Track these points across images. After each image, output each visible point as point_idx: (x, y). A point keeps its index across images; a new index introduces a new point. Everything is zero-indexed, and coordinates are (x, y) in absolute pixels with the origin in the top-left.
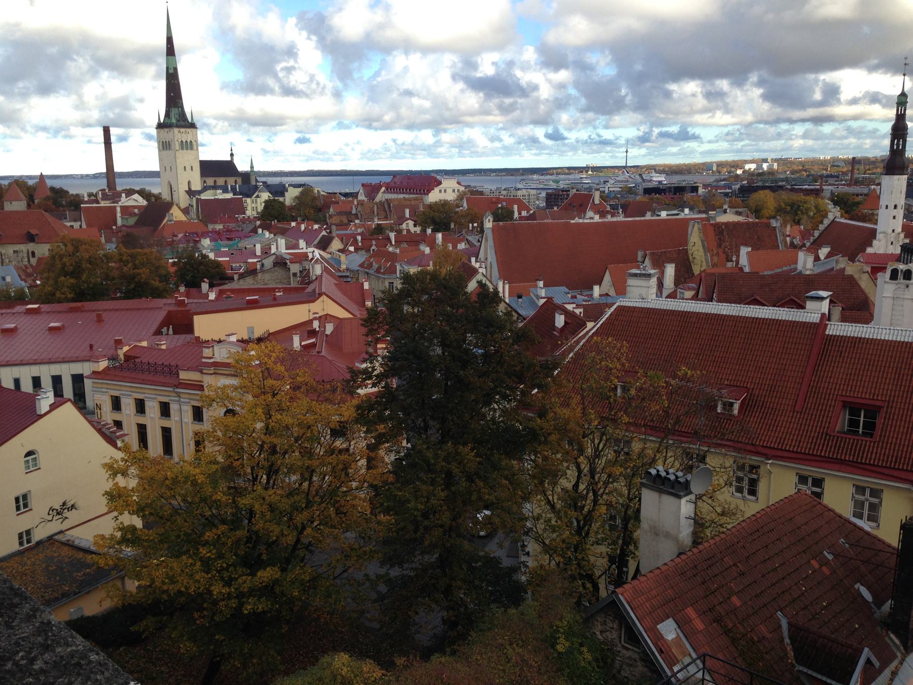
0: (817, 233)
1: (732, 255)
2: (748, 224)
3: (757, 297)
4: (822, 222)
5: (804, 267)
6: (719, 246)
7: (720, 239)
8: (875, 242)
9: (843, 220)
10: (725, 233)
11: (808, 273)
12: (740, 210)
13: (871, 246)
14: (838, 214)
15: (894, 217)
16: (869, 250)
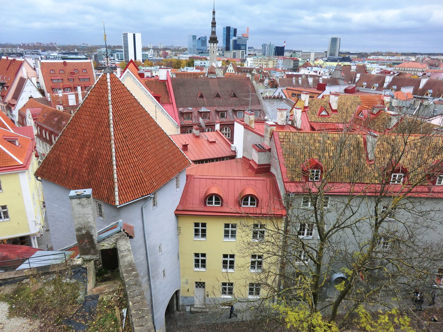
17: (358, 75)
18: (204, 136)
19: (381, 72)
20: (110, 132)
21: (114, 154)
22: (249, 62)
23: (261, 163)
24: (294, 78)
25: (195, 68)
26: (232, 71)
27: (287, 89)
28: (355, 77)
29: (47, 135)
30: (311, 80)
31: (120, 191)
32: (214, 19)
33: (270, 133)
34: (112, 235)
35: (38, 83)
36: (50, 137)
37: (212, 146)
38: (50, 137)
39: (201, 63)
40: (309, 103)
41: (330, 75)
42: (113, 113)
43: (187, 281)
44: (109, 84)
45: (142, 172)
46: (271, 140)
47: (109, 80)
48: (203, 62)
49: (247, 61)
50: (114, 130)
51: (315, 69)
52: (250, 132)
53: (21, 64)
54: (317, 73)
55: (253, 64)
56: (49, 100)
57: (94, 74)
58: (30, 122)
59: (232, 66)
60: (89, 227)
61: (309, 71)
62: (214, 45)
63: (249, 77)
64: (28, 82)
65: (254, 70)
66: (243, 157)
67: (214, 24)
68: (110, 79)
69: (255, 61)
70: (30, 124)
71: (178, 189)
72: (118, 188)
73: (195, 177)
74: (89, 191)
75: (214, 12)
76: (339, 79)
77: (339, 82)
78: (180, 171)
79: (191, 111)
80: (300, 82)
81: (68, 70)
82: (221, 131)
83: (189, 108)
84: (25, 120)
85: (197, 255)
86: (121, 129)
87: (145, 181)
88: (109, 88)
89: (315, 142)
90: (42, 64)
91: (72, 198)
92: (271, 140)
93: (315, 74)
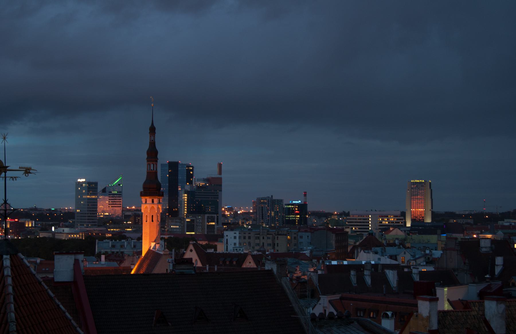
17: (499, 260)
22: (231, 241)
24: (352, 273)
25: (103, 257)
27: (341, 299)
28: (494, 265)
30: (392, 276)
32: (152, 144)
39: (113, 246)
40: (439, 323)
41: (427, 263)
47: (7, 272)
48: (118, 243)
49: (226, 238)
51: (391, 250)
54: (396, 259)
55: (240, 244)
59: (194, 251)
61: (378, 256)
62: (153, 202)
63: (272, 270)
65: (249, 259)
68: (12, 270)
69: (245, 238)
75: (153, 130)
80: (368, 280)
88: (10, 289)
93: (394, 262)
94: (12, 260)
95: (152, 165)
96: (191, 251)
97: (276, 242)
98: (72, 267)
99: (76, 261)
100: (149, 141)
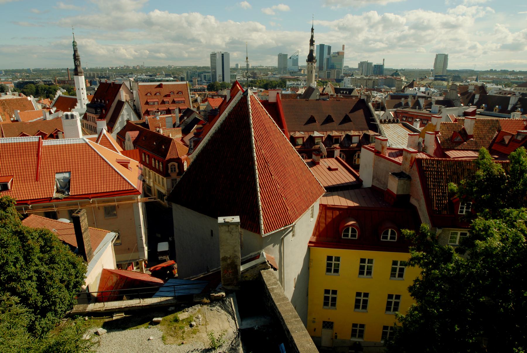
0: (54, 102)
1: (12, 115)
2: (16, 99)
3: (24, 133)
4: (55, 97)
5: (46, 117)
6: (4, 111)
7: (3, 107)
8: (77, 104)
9: (63, 95)
10: (6, 104)
11: (48, 119)
12: (14, 93)
13: (76, 105)
14: (61, 94)
15: (83, 93)
16: (76, 107)
17: (477, 96)
18: (325, 163)
19: (500, 93)
20: (252, 158)
21: (258, 180)
22: (347, 82)
23: (400, 193)
25: (290, 89)
26: (329, 92)
29: (147, 159)
30: (422, 102)
31: (264, 219)
32: (312, 37)
33: (411, 161)
34: (256, 266)
35: (134, 105)
36: (150, 161)
37: (334, 172)
38: (150, 161)
42: (254, 137)
43: (314, 320)
44: (250, 107)
45: (284, 200)
46: (411, 168)
49: (344, 81)
50: (257, 155)
52: (383, 159)
53: (120, 86)
56: (147, 123)
57: (190, 96)
58: (129, 145)
60: (235, 257)
62: (312, 64)
63: (364, 99)
64: (126, 106)
66: (372, 185)
67: (312, 42)
68: (251, 102)
70: (129, 147)
71: (312, 219)
72: (263, 216)
73: (328, 206)
74: (237, 219)
75: (312, 30)
76: (455, 99)
77: (454, 104)
78: (315, 200)
79: (303, 136)
81: (165, 92)
82: (340, 156)
83: (301, 132)
84: (124, 144)
85: (327, 291)
86: (263, 154)
87: (288, 210)
89: (464, 171)
90: (139, 86)
91: (221, 224)
92: (411, 168)
94: (251, 98)
95: (312, 47)
96: (328, 87)
97: (368, 83)
98: (276, 96)
99: (278, 93)
100: (311, 35)
